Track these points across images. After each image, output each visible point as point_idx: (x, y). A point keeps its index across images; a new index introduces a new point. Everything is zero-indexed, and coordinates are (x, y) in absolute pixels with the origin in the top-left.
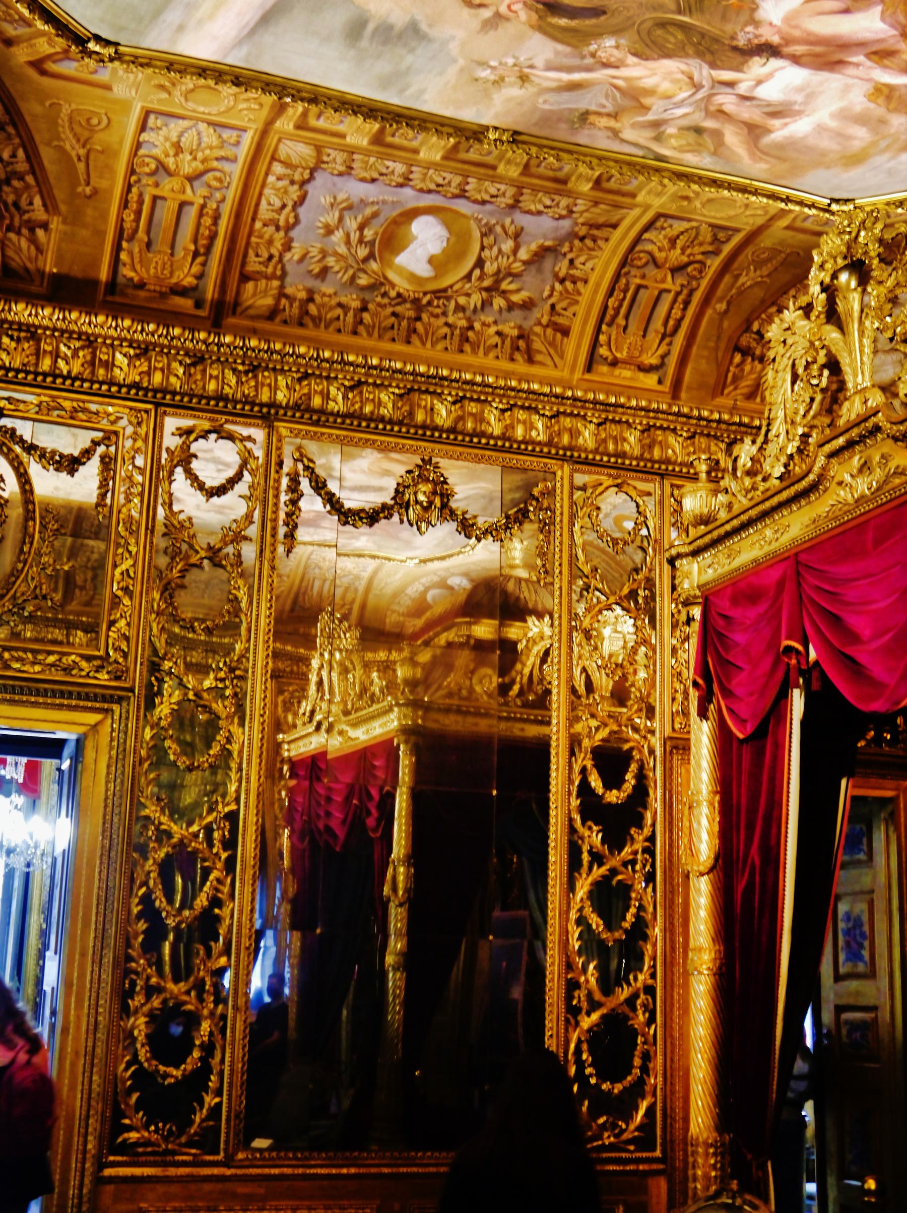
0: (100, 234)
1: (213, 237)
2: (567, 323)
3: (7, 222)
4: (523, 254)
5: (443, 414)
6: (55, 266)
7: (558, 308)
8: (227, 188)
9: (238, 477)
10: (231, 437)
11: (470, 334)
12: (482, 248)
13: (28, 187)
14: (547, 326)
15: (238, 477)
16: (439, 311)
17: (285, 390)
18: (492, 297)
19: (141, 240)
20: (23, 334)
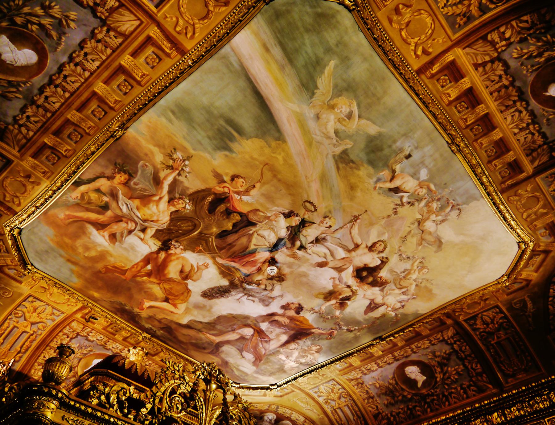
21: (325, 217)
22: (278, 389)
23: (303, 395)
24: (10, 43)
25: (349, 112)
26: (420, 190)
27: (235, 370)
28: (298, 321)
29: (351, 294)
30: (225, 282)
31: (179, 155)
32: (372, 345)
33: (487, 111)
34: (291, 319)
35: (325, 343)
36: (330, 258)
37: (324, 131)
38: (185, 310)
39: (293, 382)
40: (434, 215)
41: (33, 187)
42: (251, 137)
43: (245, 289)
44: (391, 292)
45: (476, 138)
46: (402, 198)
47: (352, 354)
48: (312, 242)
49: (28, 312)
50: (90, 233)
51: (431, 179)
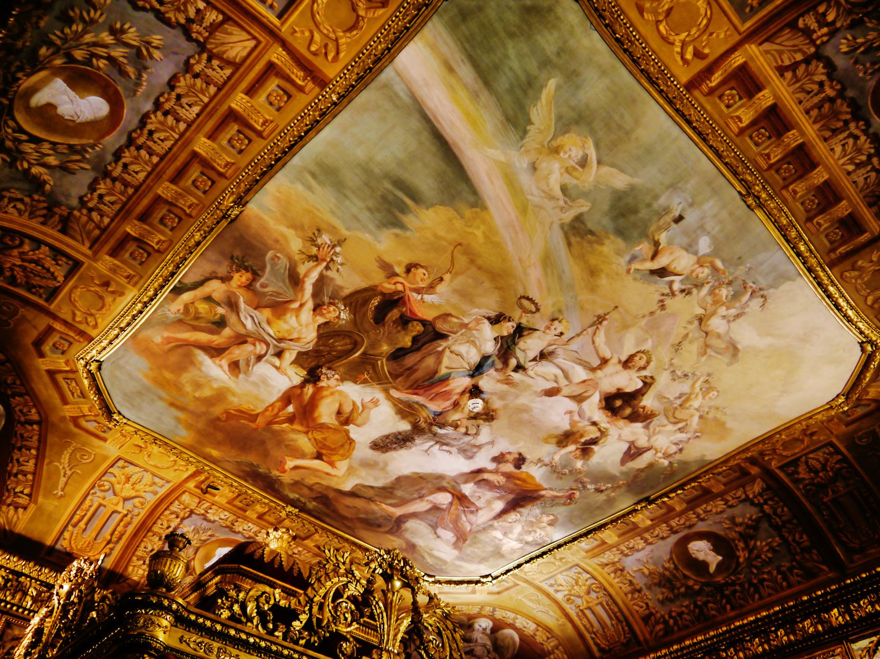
21: (553, 320)
22: (494, 582)
23: (532, 590)
24: (68, 89)
25: (583, 157)
26: (700, 270)
27: (427, 556)
28: (519, 479)
29: (598, 434)
30: (405, 426)
31: (325, 239)
32: (635, 511)
33: (802, 140)
34: (508, 476)
35: (561, 511)
36: (563, 382)
37: (545, 188)
38: (348, 470)
39: (516, 571)
40: (724, 308)
41: (115, 299)
42: (432, 205)
43: (435, 434)
44: (661, 428)
45: (787, 183)
46: (671, 283)
47: (604, 526)
48: (534, 359)
49: (119, 483)
50: (201, 363)
51: (716, 252)
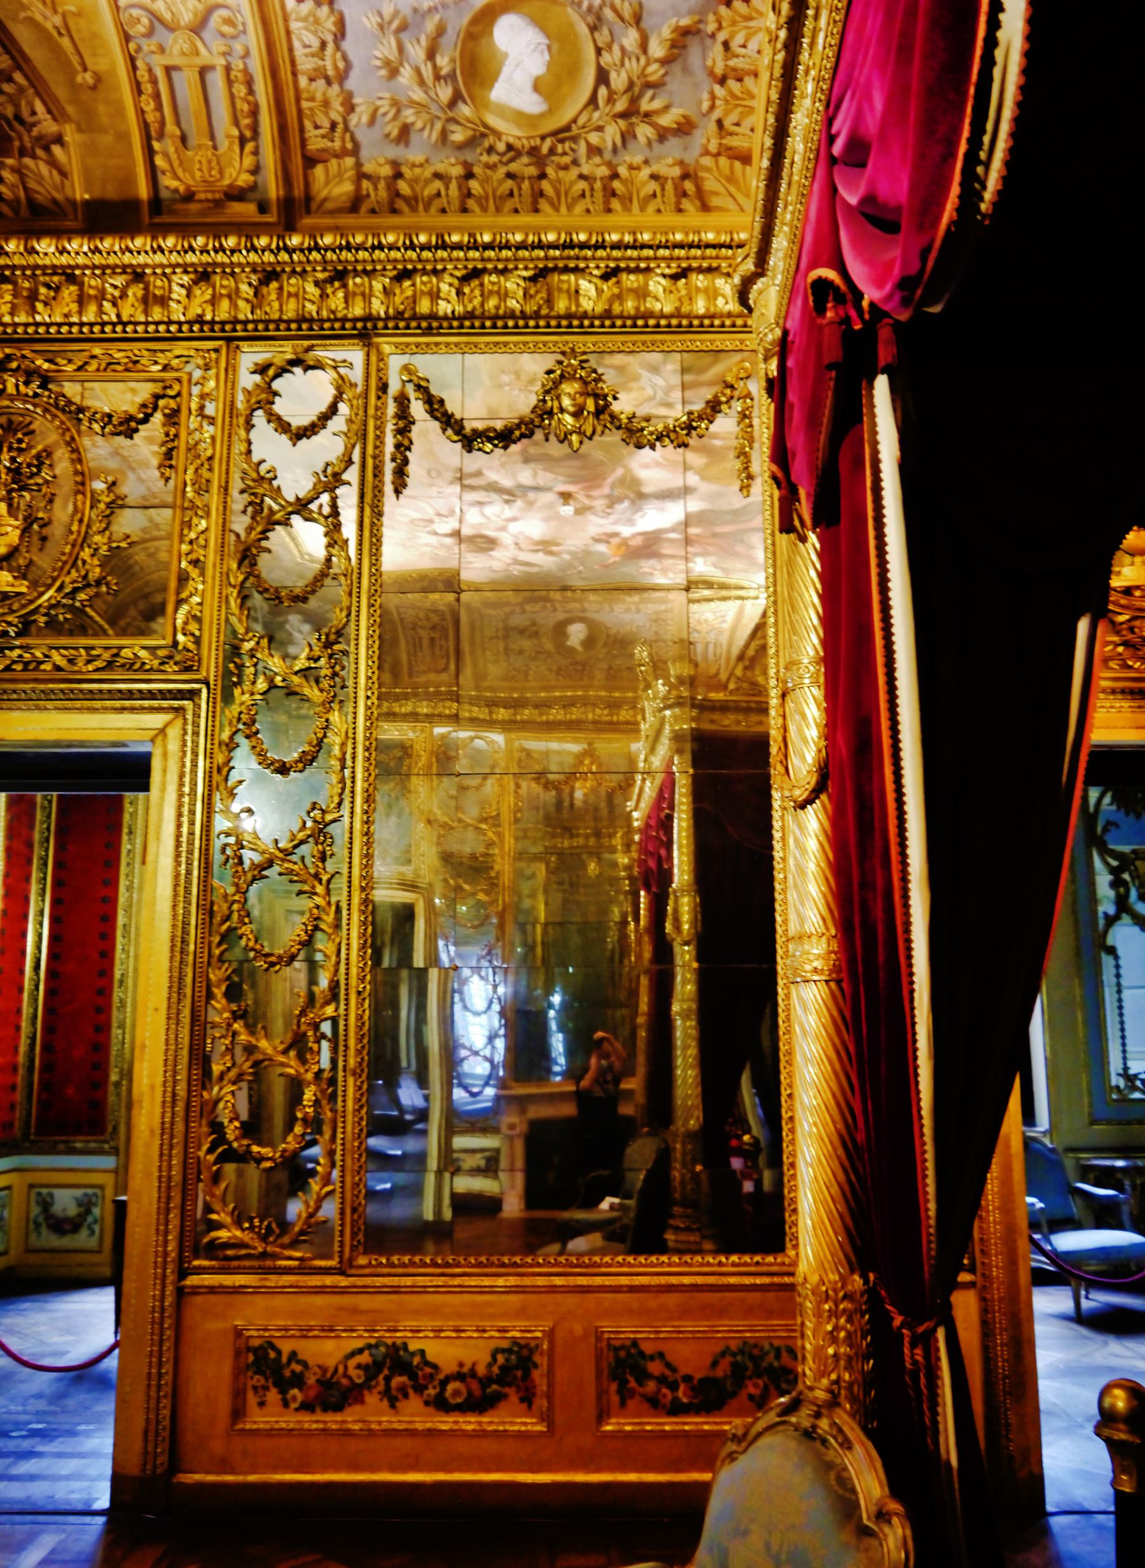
0: (123, 137)
1: (254, 113)
2: (746, 145)
3: (17, 144)
4: (657, 50)
5: (590, 294)
6: (87, 191)
7: (727, 123)
8: (244, 32)
9: (333, 410)
10: (318, 366)
11: (616, 184)
12: (599, 51)
13: (21, 90)
14: (718, 154)
15: (333, 410)
16: (566, 160)
17: (381, 296)
18: (632, 124)
19: (173, 136)
20: (56, 279)
24: (502, 78)
